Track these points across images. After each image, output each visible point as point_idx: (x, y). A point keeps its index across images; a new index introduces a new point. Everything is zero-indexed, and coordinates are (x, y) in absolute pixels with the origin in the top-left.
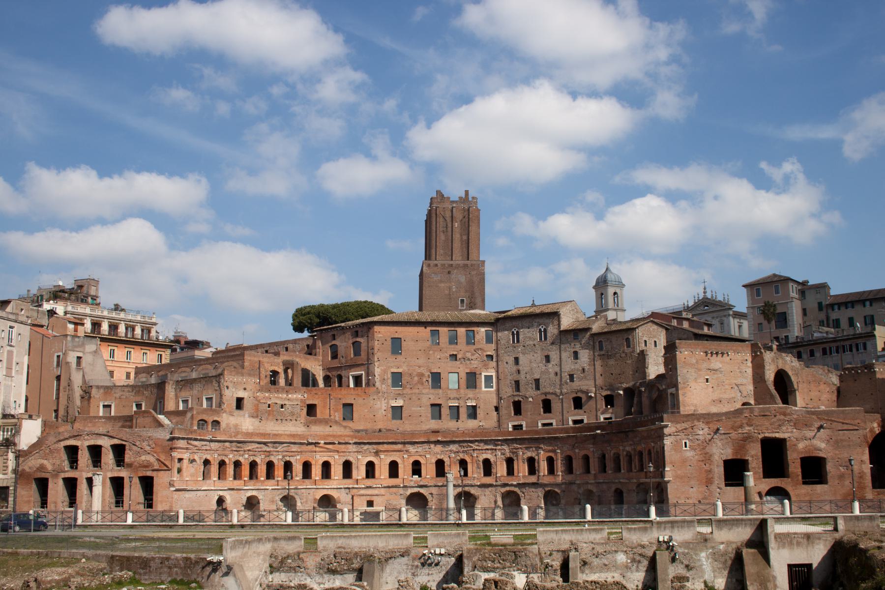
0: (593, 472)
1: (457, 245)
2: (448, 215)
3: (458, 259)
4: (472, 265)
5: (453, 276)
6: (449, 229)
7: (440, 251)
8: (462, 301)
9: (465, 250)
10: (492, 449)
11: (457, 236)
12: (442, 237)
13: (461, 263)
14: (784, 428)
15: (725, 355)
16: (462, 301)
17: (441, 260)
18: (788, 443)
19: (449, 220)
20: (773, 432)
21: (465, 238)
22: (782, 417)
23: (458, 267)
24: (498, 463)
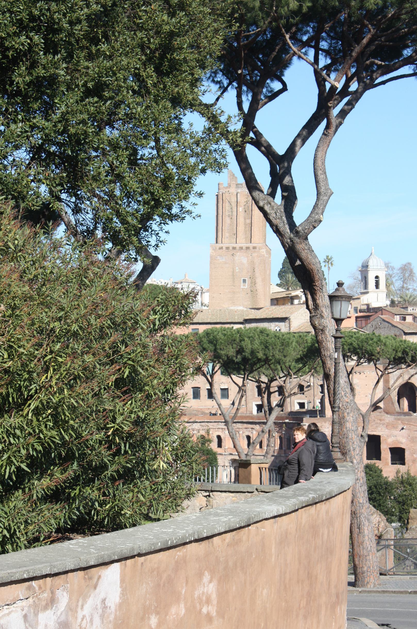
0: (284, 449)
1: (241, 228)
2: (234, 200)
3: (242, 242)
4: (254, 248)
5: (236, 258)
6: (235, 213)
7: (226, 234)
8: (244, 281)
9: (249, 233)
10: (222, 429)
11: (241, 220)
12: (227, 221)
13: (244, 245)
14: (380, 429)
15: (362, 374)
16: (244, 281)
17: (227, 242)
18: (381, 439)
19: (234, 205)
20: (372, 431)
21: (248, 221)
22: (379, 421)
23: (241, 248)
24: (227, 439)
